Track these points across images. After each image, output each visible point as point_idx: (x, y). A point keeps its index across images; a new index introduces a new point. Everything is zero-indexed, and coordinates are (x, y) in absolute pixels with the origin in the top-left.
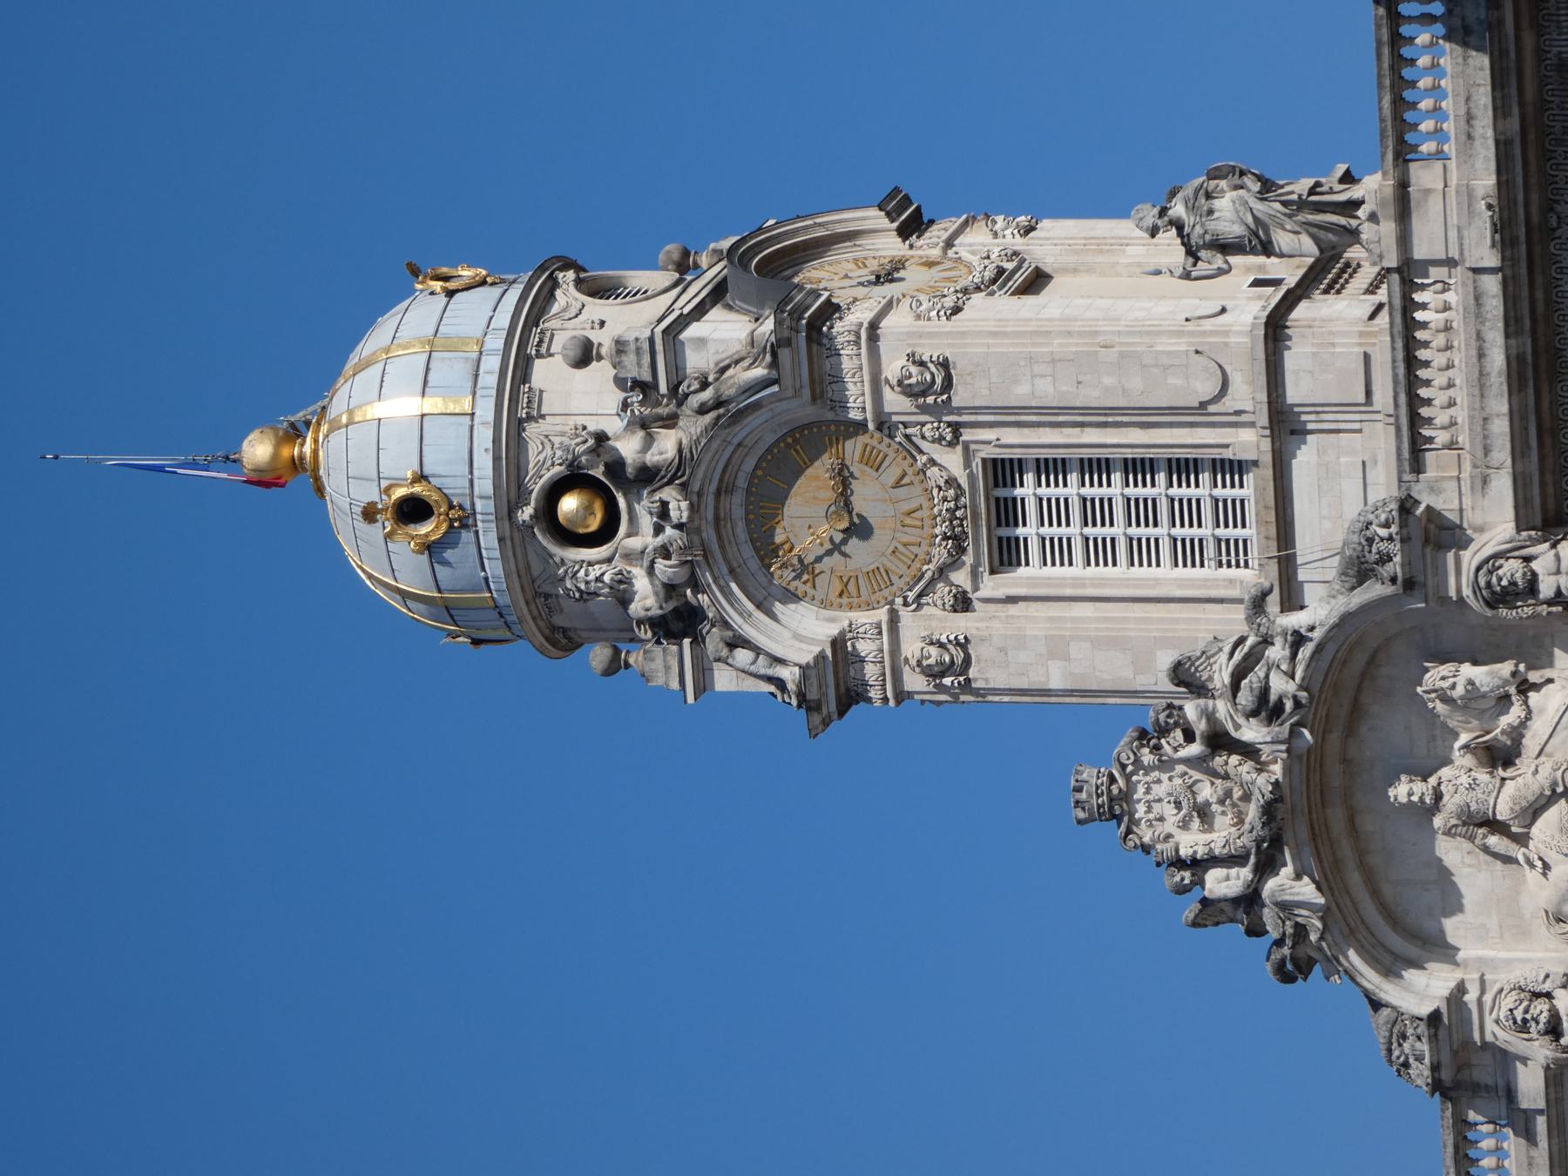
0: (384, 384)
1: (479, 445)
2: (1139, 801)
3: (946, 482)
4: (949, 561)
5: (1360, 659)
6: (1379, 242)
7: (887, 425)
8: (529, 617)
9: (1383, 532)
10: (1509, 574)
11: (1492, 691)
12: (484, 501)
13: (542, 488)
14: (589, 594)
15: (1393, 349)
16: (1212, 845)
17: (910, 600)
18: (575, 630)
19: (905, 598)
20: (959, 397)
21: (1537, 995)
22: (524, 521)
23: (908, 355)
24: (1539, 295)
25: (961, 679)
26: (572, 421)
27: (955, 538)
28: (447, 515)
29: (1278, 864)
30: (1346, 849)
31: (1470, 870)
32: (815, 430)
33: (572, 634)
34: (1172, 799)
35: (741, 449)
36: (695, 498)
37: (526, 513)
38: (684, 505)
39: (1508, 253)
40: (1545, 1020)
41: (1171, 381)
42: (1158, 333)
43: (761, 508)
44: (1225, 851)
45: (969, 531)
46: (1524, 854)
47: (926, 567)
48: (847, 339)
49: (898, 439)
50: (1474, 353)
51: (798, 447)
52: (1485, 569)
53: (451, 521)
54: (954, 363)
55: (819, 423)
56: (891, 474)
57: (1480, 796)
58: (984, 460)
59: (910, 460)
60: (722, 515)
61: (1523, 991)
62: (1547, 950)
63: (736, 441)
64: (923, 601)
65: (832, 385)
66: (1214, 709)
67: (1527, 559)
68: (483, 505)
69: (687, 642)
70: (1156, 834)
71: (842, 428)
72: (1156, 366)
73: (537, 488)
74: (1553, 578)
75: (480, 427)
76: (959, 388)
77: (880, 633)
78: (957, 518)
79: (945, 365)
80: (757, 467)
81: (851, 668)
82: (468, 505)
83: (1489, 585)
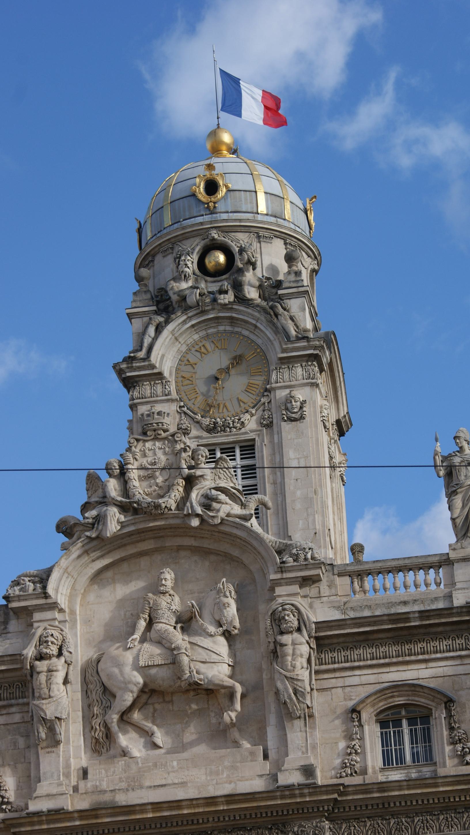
2: (154, 445)
3: (243, 422)
4: (204, 426)
5: (236, 553)
6: (462, 548)
7: (269, 394)
9: (309, 556)
10: (291, 620)
11: (224, 616)
13: (227, 242)
14: (179, 261)
15: (404, 558)
16: (134, 480)
17: (183, 409)
18: (153, 266)
19: (183, 407)
20: (286, 427)
21: (60, 650)
22: (210, 234)
24: (440, 629)
26: (258, 256)
27: (215, 428)
28: (211, 202)
29: (125, 514)
30: (131, 550)
31: (123, 616)
32: (264, 362)
33: (151, 264)
34: (157, 461)
35: (254, 328)
36: (230, 306)
37: (215, 234)
38: (226, 301)
39: (464, 610)
40: (48, 652)
41: (301, 522)
42: (323, 516)
44: (132, 487)
45: (219, 434)
46: (137, 638)
47: (200, 415)
48: (311, 374)
49: (262, 399)
50: (406, 599)
52: (294, 608)
53: (208, 204)
54: (303, 422)
56: (244, 397)
57: (166, 615)
58: (254, 440)
59: (252, 405)
60: (220, 321)
61: (62, 642)
62: (82, 656)
63: (258, 325)
64: (183, 415)
66: (206, 479)
67: (299, 630)
69: (154, 308)
70: (137, 454)
72: (308, 515)
73: (227, 240)
74: (290, 642)
76: (290, 425)
77: (166, 395)
78: (225, 428)
79: (302, 418)
83: (284, 610)
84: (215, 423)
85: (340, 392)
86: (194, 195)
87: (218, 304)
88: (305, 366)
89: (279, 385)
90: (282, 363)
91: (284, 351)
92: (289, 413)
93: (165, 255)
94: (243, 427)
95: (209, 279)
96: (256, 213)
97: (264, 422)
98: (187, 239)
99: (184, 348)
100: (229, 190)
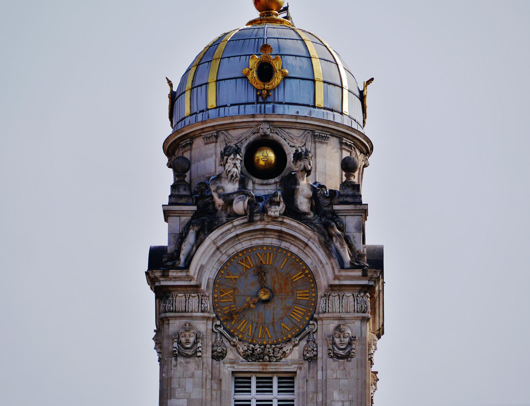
0: (326, 62)
1: (300, 108)
3: (284, 352)
7: (315, 323)
8: (205, 126)
12: (271, 108)
14: (227, 159)
17: (219, 328)
18: (191, 150)
23: (355, 337)
25: (177, 353)
27: (252, 354)
32: (312, 285)
35: (304, 246)
36: (280, 219)
43: (270, 254)
51: (303, 276)
53: (262, 90)
54: (350, 361)
55: (316, 287)
58: (295, 373)
63: (310, 243)
64: (218, 335)
65: (338, 297)
68: (269, 108)
71: (313, 300)
75: (309, 110)
76: (336, 363)
77: (202, 312)
78: (264, 356)
80: (292, 253)
81: (182, 294)
82: (269, 100)
84: (253, 350)
85: (377, 303)
86: (245, 77)
87: (267, 215)
88: (357, 296)
89: (326, 315)
90: (332, 290)
91: (336, 278)
92: (336, 349)
93: (208, 141)
94: (285, 357)
95: (257, 180)
96: (312, 106)
97: (308, 355)
98: (234, 129)
99: (225, 258)
100: (286, 77)
